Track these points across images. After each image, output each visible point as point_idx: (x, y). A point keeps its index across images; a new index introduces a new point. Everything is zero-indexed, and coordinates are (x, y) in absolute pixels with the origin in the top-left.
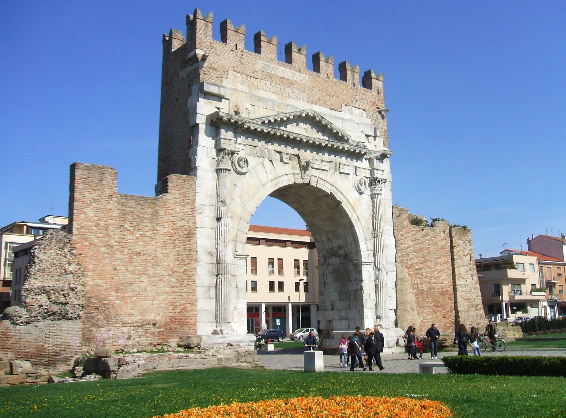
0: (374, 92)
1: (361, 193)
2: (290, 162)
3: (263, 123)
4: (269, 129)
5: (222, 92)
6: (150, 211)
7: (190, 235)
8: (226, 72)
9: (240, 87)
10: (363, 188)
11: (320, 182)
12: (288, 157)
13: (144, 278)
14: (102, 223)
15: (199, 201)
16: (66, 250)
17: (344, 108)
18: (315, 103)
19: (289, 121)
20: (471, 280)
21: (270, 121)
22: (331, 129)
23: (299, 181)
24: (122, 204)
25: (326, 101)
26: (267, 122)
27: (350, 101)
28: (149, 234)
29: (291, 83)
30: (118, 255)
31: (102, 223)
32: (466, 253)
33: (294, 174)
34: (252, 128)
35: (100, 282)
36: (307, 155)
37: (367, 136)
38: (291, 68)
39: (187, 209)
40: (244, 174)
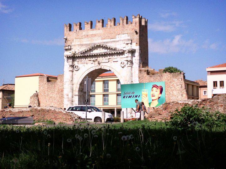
0: (133, 25)
1: (123, 67)
2: (94, 62)
3: (81, 53)
4: (83, 55)
5: (70, 48)
6: (53, 86)
7: (62, 91)
8: (73, 40)
9: (77, 43)
10: (123, 66)
11: (105, 66)
12: (92, 61)
13: (52, 103)
14: (44, 90)
15: (65, 80)
16: (35, 98)
17: (117, 36)
18: (105, 39)
19: (91, 50)
20: (181, 97)
21: (83, 52)
22: (107, 47)
23: (97, 68)
24: (48, 85)
25: (109, 37)
26: (82, 53)
27: (120, 32)
28: (53, 92)
29: (95, 35)
30: (47, 98)
31: (44, 90)
32: (178, 84)
33: (95, 66)
34: (77, 56)
35: (44, 105)
36: (100, 59)
37: (127, 44)
38: (96, 30)
39: (62, 84)
40: (78, 70)
